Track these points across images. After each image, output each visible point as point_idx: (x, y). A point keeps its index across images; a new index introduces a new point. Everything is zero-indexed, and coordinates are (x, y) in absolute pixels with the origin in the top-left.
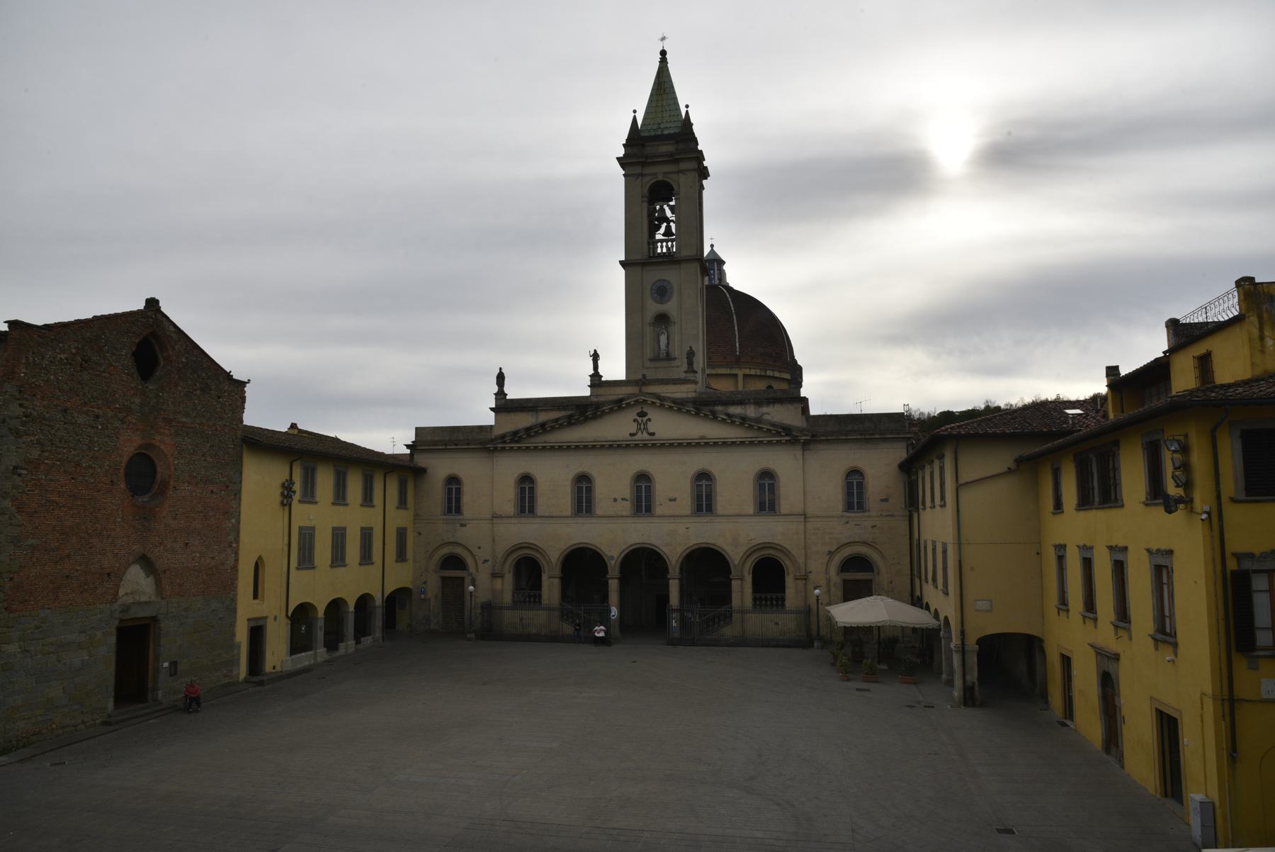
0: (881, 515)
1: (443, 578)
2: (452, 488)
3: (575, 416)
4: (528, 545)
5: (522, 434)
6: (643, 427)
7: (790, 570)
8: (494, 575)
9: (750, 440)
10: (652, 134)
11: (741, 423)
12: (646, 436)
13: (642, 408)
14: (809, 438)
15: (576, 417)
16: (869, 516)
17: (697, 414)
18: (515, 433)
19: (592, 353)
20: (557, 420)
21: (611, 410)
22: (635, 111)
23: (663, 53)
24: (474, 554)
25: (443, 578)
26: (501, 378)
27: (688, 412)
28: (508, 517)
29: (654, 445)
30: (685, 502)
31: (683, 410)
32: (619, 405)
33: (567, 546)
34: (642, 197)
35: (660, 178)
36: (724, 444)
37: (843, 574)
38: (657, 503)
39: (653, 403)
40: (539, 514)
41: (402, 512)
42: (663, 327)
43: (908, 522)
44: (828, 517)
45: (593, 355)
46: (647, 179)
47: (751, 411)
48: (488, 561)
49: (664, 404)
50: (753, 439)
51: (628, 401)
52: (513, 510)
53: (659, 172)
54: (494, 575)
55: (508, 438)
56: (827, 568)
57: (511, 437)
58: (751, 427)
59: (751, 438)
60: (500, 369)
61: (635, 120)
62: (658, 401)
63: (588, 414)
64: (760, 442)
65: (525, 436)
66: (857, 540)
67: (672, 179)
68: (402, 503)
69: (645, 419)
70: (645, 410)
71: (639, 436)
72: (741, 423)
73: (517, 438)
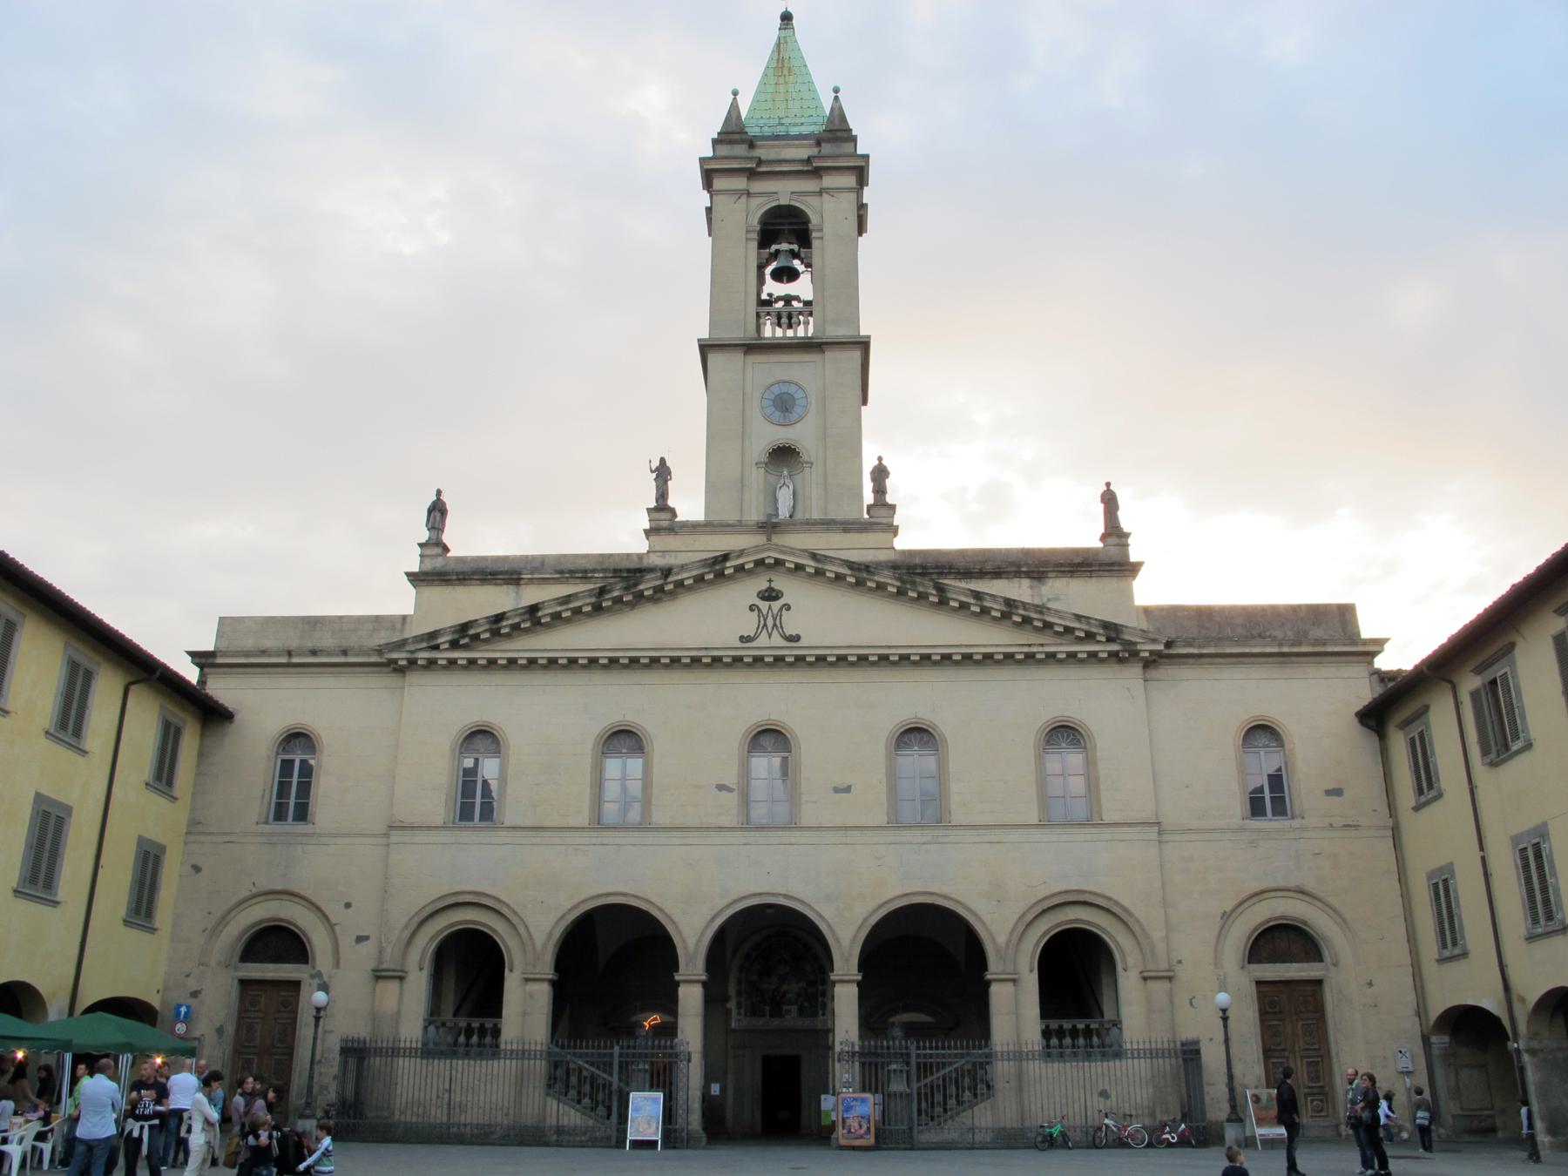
0: (1331, 826)
1: (245, 984)
2: (292, 761)
3: (610, 591)
4: (475, 899)
5: (480, 630)
7: (1130, 962)
8: (379, 975)
9: (1026, 649)
10: (767, 131)
11: (1003, 613)
12: (777, 640)
13: (770, 581)
14: (1161, 647)
15: (616, 594)
16: (1303, 829)
17: (901, 593)
18: (464, 628)
19: (656, 464)
20: (567, 599)
21: (699, 579)
22: (735, 93)
23: (787, 18)
24: (333, 919)
25: (245, 984)
26: (438, 512)
27: (881, 587)
28: (429, 828)
29: (800, 659)
30: (870, 803)
31: (869, 584)
32: (718, 570)
33: (574, 901)
34: (747, 232)
35: (784, 201)
36: (967, 658)
37: (1253, 967)
38: (804, 798)
39: (799, 567)
40: (507, 823)
41: (159, 802)
42: (786, 473)
43: (1391, 840)
44: (1212, 830)
45: (657, 469)
46: (755, 202)
47: (1020, 590)
48: (367, 938)
49: (818, 570)
50: (1034, 649)
51: (740, 561)
52: (442, 811)
53: (784, 192)
54: (379, 975)
55: (448, 638)
56: (1216, 951)
58: (1027, 621)
59: (1030, 645)
60: (439, 493)
61: (734, 107)
62: (812, 563)
63: (641, 587)
64: (1051, 656)
66: (1282, 883)
67: (810, 206)
68: (164, 775)
69: (776, 605)
70: (776, 585)
71: (763, 640)
72: (1003, 613)
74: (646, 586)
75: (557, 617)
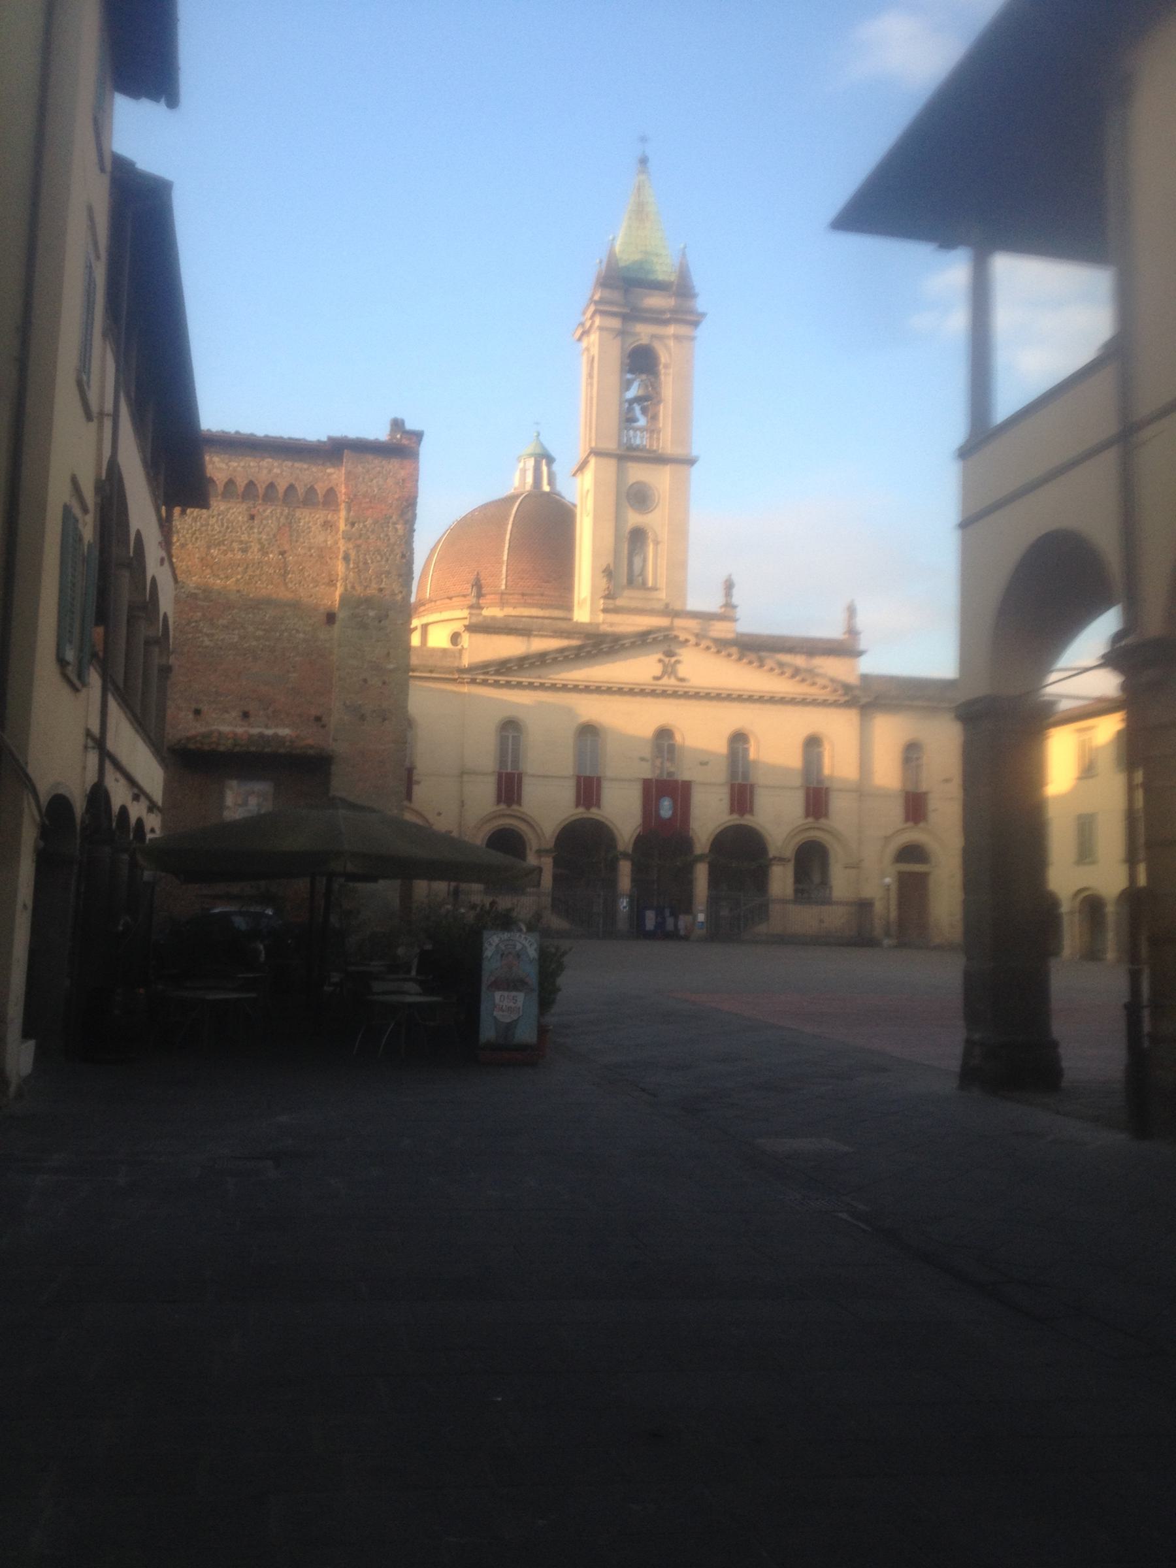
5: (512, 665)
6: (669, 670)
12: (673, 681)
47: (800, 661)
57: (497, 668)
65: (516, 668)
69: (673, 659)
73: (504, 670)
74: (605, 646)
75: (555, 660)
